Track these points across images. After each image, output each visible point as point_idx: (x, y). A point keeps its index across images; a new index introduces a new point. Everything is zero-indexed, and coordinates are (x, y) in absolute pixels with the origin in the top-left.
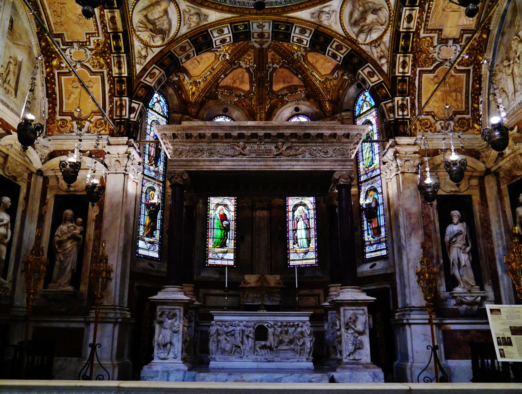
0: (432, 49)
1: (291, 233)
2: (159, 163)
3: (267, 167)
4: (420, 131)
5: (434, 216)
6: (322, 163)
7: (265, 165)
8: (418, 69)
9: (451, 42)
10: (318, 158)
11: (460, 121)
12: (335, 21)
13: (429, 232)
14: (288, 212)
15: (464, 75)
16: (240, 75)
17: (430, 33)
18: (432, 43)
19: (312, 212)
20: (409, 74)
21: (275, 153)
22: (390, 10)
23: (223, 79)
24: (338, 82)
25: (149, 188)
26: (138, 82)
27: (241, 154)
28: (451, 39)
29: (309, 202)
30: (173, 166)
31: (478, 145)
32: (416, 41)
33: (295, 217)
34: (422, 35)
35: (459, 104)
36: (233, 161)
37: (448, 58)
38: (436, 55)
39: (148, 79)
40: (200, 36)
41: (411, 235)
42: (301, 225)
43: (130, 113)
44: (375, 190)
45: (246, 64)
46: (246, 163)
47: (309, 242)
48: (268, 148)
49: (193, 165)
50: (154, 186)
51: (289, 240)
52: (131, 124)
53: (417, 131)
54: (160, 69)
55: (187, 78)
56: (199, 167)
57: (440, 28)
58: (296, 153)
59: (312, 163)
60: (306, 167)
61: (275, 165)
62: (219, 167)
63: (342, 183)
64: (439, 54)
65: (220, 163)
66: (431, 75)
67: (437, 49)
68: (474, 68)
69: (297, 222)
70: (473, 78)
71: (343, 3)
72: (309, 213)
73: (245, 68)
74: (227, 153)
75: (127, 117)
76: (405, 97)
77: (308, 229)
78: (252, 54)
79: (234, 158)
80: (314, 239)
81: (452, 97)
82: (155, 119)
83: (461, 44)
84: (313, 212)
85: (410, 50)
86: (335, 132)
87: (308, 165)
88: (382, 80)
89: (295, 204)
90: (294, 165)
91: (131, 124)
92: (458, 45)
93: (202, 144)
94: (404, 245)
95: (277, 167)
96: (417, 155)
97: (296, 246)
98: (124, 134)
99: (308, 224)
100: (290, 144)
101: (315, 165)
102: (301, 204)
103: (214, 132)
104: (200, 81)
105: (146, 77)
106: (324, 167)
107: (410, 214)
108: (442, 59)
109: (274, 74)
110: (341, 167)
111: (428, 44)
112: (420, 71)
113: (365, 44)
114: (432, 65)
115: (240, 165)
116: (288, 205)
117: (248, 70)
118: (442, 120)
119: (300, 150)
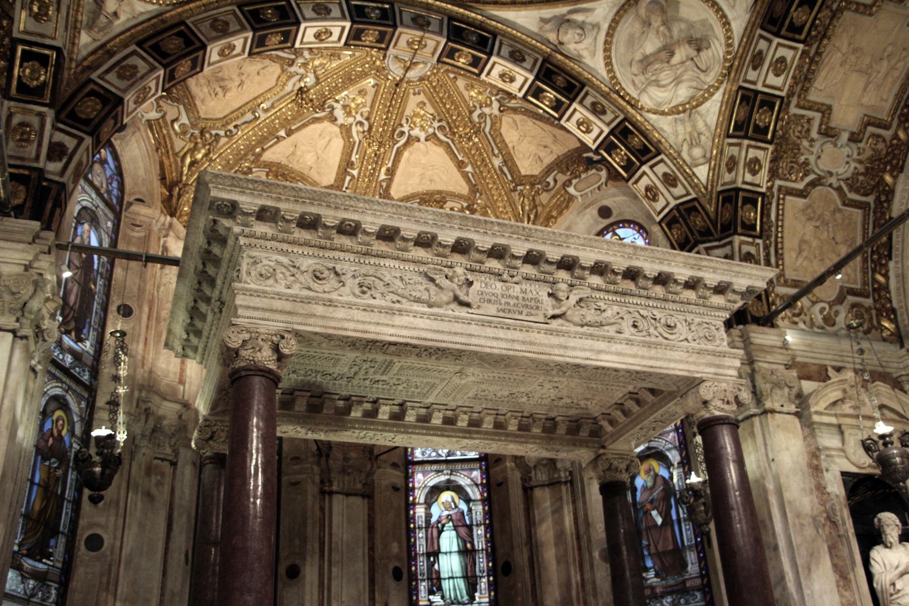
0: (805, 143)
1: (422, 564)
2: (85, 331)
3: (530, 348)
5: (844, 524)
6: (669, 354)
7: (524, 343)
8: (778, 183)
9: (845, 136)
10: (653, 339)
12: (592, 48)
13: (840, 563)
14: (414, 504)
15: (857, 214)
16: (323, 142)
17: (810, 109)
18: (808, 130)
19: (478, 510)
20: (763, 190)
21: (551, 312)
22: (729, 45)
23: (279, 139)
24: (553, 197)
25: (55, 398)
26: (84, 78)
27: (456, 299)
28: (844, 130)
29: (469, 481)
30: (248, 307)
31: (896, 365)
32: (783, 120)
33: (434, 520)
34: (793, 110)
36: (436, 317)
37: (834, 171)
38: (812, 159)
39: (112, 77)
40: (269, 8)
41: (809, 570)
42: (449, 540)
43: (50, 158)
44: (661, 457)
45: (349, 114)
46: (473, 329)
47: (472, 588)
48: (530, 296)
49: (313, 315)
50: (69, 398)
51: (417, 580)
52: (47, 190)
54: (151, 60)
55: (184, 119)
56: (333, 324)
57: (827, 102)
58: (598, 319)
59: (643, 351)
60: (631, 360)
61: (552, 346)
62: (391, 331)
63: (717, 413)
65: (398, 320)
66: (801, 202)
67: (817, 145)
68: (878, 199)
69: (440, 532)
71: (618, 12)
72: (470, 510)
73: (341, 126)
74: (418, 295)
75: (41, 165)
77: (467, 553)
78: (371, 92)
79: (435, 310)
80: (484, 580)
82: (89, 205)
84: (480, 507)
85: (769, 137)
86: (700, 274)
87: (635, 356)
88: (694, 196)
89: (431, 484)
90: (600, 352)
91: (47, 190)
93: (342, 255)
94: (795, 596)
95: (556, 351)
96: (794, 373)
97: (436, 599)
98: (27, 212)
99: (468, 539)
100: (589, 291)
101: (651, 358)
102: (449, 486)
103: (389, 223)
104: (222, 133)
105: (107, 71)
106: (672, 365)
107: (798, 515)
108: (822, 171)
109: (406, 154)
110: (712, 370)
111: (800, 132)
112: (780, 188)
113: (655, 112)
114: (802, 179)
115: (456, 334)
116: (413, 489)
117: (346, 130)
118: (825, 302)
119: (609, 313)
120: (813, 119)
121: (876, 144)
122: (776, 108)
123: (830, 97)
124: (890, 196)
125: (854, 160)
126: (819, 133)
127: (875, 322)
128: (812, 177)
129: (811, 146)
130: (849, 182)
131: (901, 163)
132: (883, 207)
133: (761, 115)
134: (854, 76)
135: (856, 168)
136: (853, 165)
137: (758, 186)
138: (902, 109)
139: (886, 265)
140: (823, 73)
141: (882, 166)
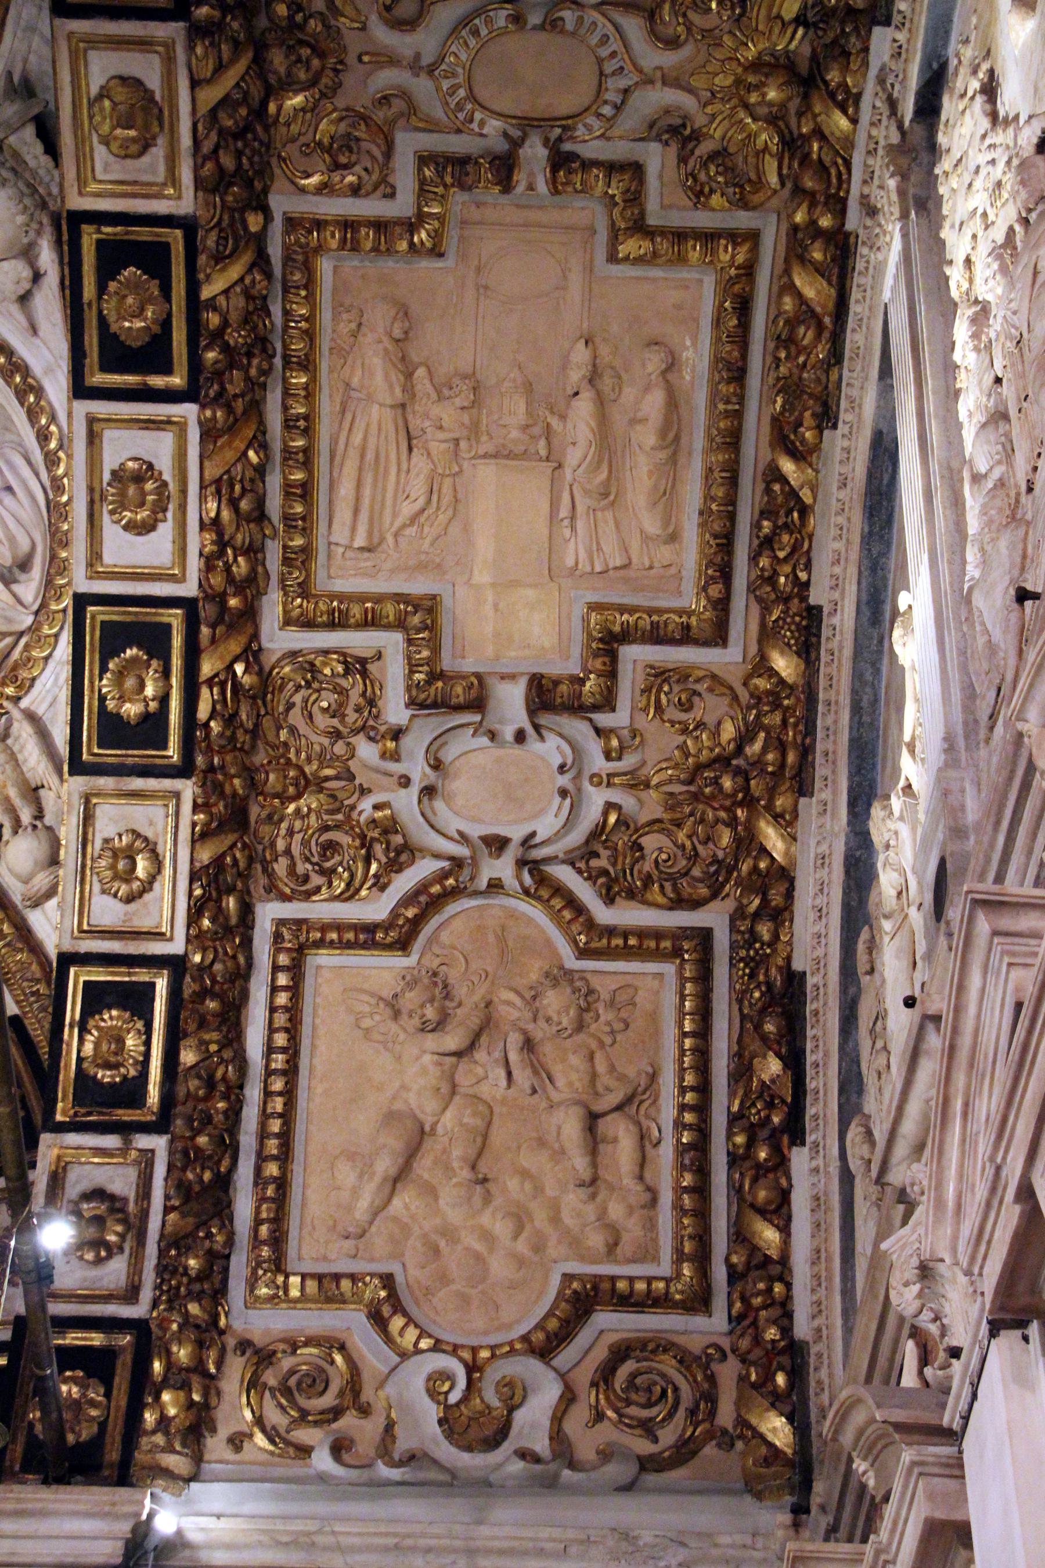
0: (367, 751)
4: (237, 1442)
11: (624, 1371)
17: (336, 622)
28: (512, 677)
35: (616, 1211)
37: (516, 833)
53: (216, 1446)
57: (418, 586)
64: (429, 791)
70: (740, 998)
76: (125, 1129)
81: (559, 1154)
83: (603, 719)
85: (173, 751)
92: (578, 728)
111: (336, 712)
114: (381, 885)
118: (455, 1350)
120: (379, 656)
121: (686, 707)
122: (177, 642)
123: (421, 567)
124: (776, 898)
125: (596, 780)
126: (411, 703)
127: (726, 1416)
128: (423, 869)
129: (395, 756)
130: (602, 862)
131: (791, 758)
132: (753, 936)
133: (120, 676)
134: (487, 473)
135: (609, 806)
136: (596, 799)
137: (158, 936)
138: (754, 559)
139: (780, 1163)
140: (346, 489)
141: (727, 783)
